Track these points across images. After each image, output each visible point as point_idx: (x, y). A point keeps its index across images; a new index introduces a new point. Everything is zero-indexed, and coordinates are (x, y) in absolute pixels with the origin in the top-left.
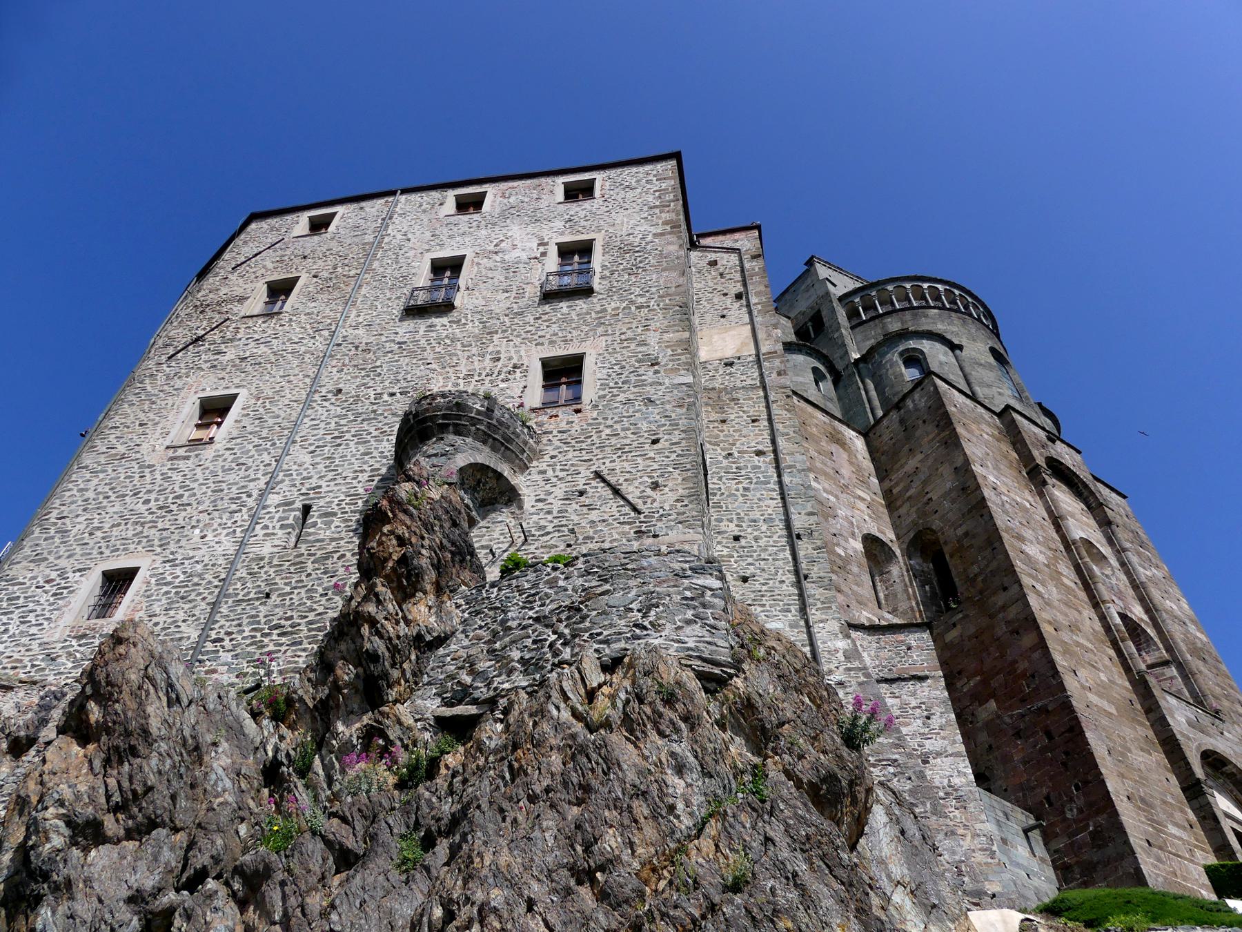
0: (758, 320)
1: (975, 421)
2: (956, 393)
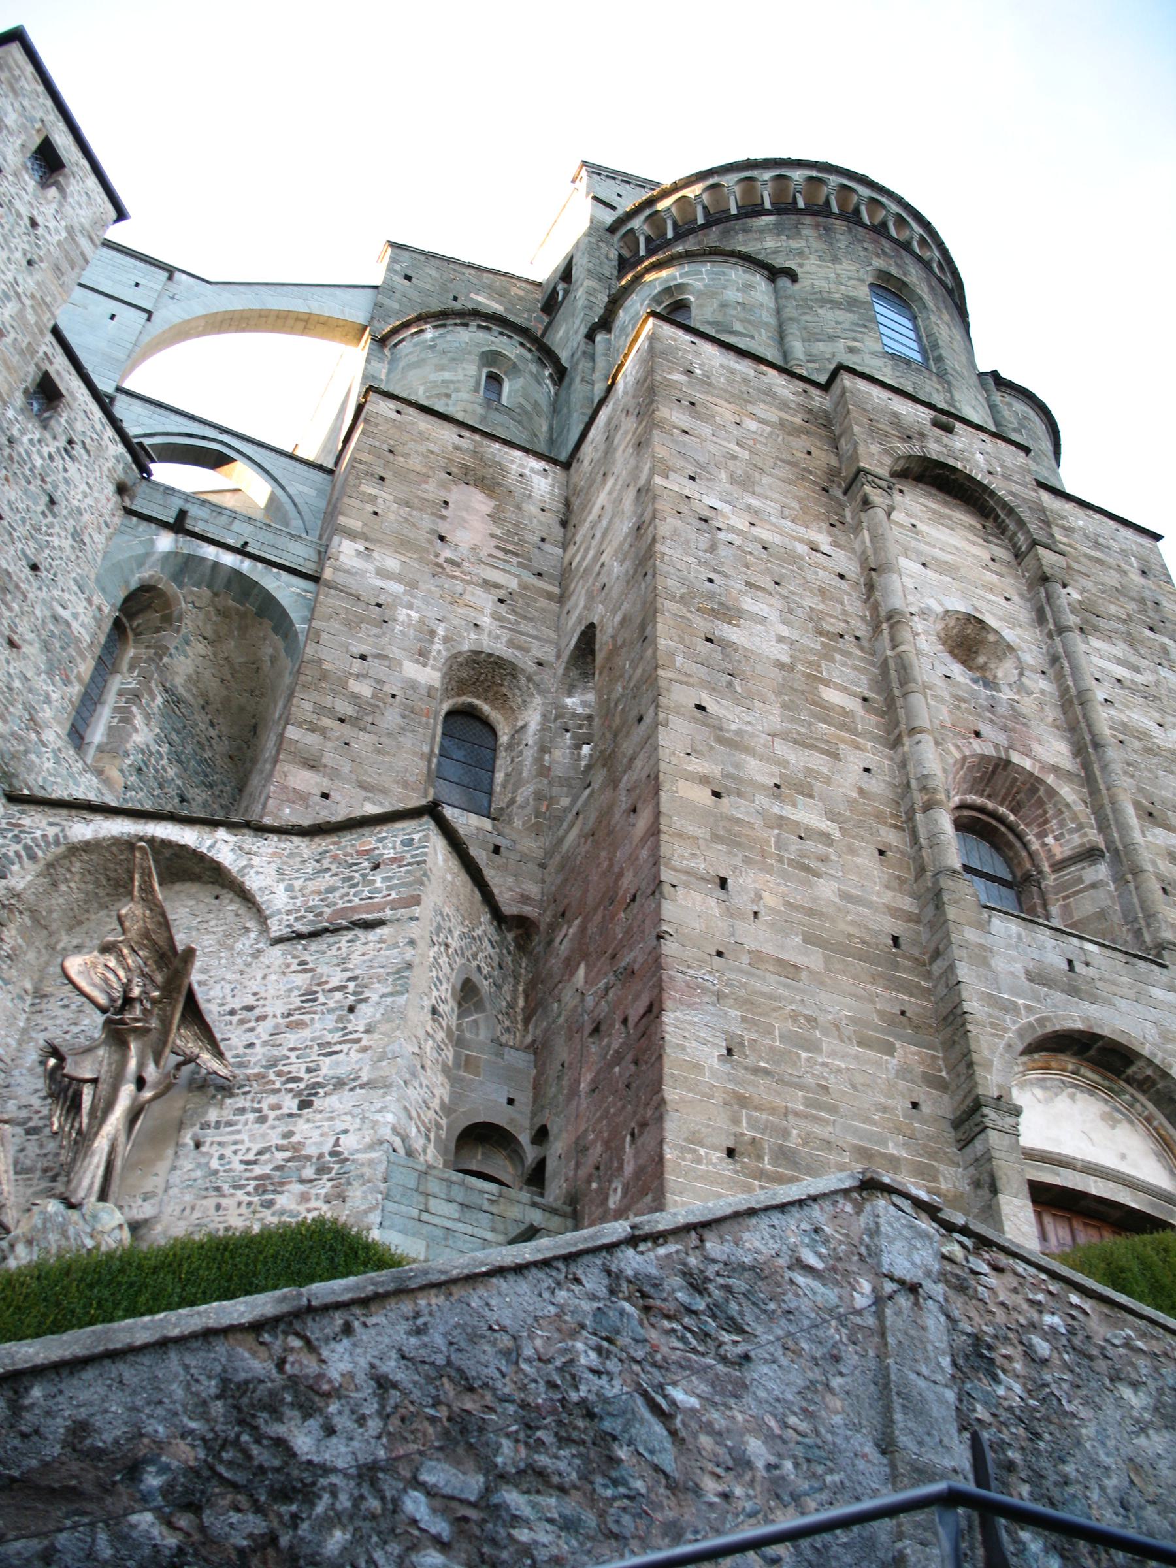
1: (741, 398)
2: (708, 348)
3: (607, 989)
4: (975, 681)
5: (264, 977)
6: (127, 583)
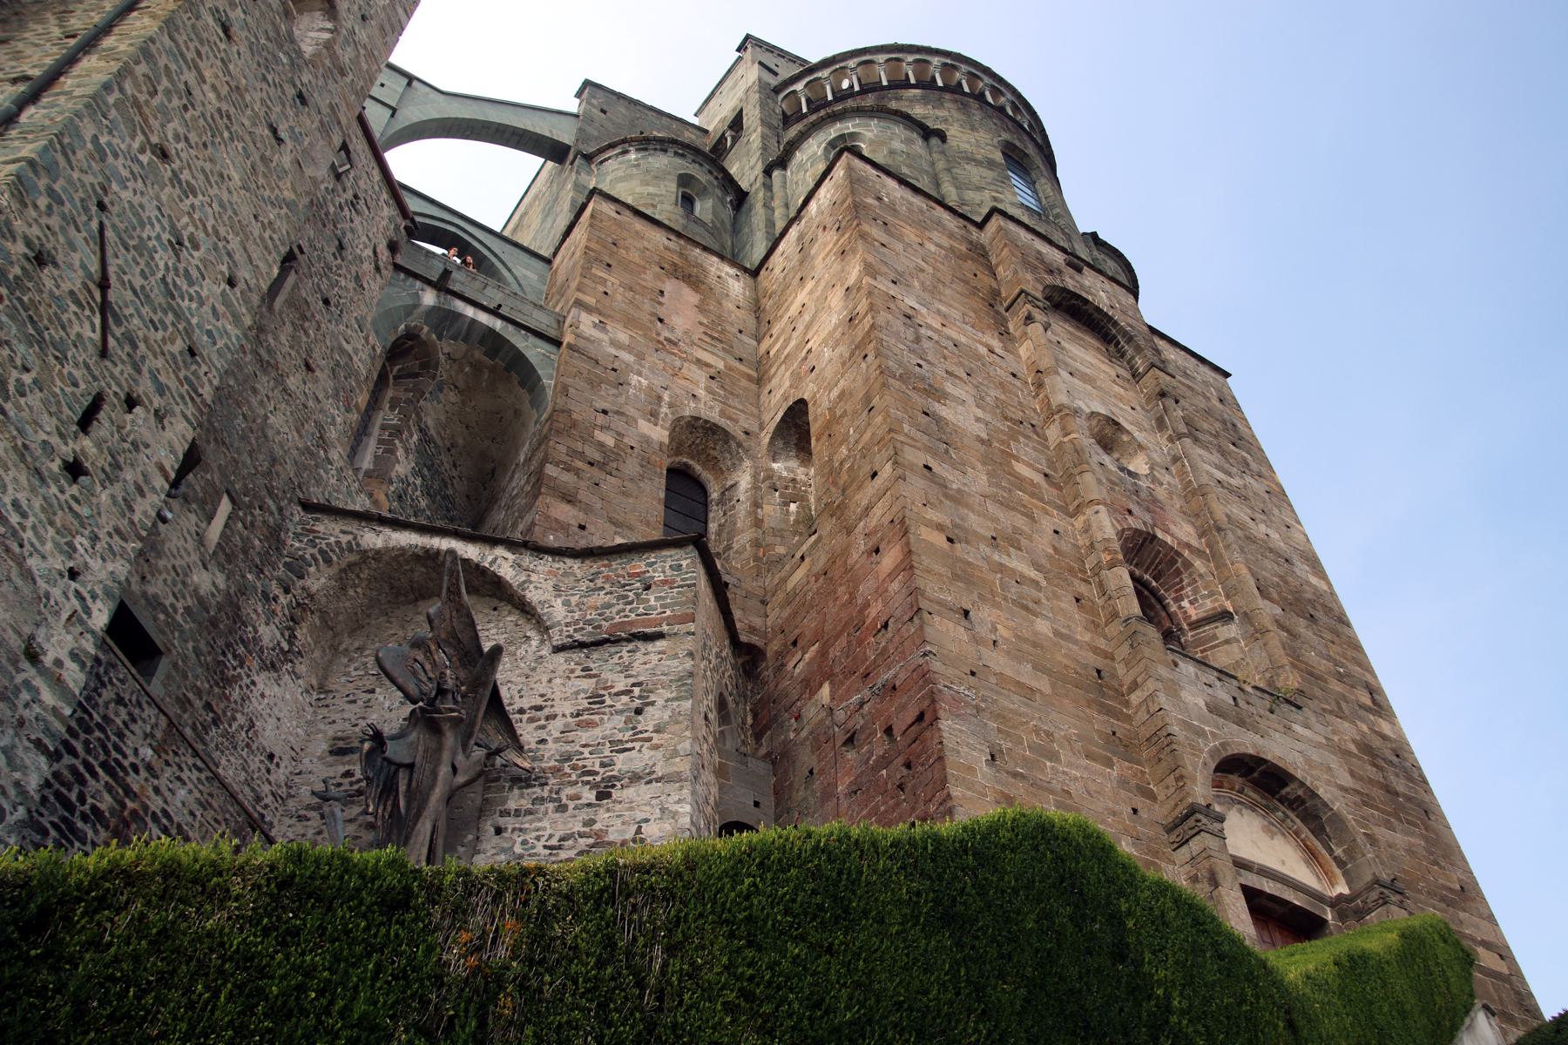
1: (922, 226)
2: (891, 183)
3: (862, 704)
4: (1122, 469)
5: (550, 681)
6: (396, 328)
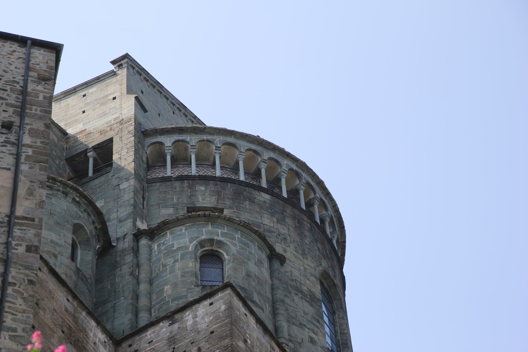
0: (24, 167)
2: (252, 321)
